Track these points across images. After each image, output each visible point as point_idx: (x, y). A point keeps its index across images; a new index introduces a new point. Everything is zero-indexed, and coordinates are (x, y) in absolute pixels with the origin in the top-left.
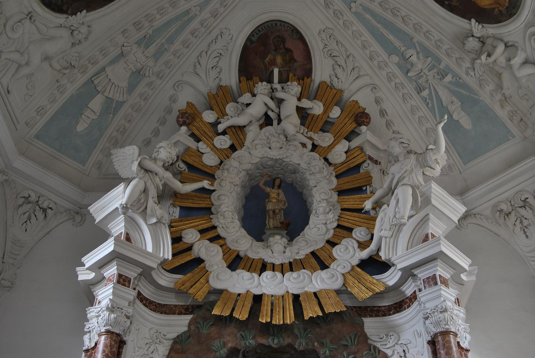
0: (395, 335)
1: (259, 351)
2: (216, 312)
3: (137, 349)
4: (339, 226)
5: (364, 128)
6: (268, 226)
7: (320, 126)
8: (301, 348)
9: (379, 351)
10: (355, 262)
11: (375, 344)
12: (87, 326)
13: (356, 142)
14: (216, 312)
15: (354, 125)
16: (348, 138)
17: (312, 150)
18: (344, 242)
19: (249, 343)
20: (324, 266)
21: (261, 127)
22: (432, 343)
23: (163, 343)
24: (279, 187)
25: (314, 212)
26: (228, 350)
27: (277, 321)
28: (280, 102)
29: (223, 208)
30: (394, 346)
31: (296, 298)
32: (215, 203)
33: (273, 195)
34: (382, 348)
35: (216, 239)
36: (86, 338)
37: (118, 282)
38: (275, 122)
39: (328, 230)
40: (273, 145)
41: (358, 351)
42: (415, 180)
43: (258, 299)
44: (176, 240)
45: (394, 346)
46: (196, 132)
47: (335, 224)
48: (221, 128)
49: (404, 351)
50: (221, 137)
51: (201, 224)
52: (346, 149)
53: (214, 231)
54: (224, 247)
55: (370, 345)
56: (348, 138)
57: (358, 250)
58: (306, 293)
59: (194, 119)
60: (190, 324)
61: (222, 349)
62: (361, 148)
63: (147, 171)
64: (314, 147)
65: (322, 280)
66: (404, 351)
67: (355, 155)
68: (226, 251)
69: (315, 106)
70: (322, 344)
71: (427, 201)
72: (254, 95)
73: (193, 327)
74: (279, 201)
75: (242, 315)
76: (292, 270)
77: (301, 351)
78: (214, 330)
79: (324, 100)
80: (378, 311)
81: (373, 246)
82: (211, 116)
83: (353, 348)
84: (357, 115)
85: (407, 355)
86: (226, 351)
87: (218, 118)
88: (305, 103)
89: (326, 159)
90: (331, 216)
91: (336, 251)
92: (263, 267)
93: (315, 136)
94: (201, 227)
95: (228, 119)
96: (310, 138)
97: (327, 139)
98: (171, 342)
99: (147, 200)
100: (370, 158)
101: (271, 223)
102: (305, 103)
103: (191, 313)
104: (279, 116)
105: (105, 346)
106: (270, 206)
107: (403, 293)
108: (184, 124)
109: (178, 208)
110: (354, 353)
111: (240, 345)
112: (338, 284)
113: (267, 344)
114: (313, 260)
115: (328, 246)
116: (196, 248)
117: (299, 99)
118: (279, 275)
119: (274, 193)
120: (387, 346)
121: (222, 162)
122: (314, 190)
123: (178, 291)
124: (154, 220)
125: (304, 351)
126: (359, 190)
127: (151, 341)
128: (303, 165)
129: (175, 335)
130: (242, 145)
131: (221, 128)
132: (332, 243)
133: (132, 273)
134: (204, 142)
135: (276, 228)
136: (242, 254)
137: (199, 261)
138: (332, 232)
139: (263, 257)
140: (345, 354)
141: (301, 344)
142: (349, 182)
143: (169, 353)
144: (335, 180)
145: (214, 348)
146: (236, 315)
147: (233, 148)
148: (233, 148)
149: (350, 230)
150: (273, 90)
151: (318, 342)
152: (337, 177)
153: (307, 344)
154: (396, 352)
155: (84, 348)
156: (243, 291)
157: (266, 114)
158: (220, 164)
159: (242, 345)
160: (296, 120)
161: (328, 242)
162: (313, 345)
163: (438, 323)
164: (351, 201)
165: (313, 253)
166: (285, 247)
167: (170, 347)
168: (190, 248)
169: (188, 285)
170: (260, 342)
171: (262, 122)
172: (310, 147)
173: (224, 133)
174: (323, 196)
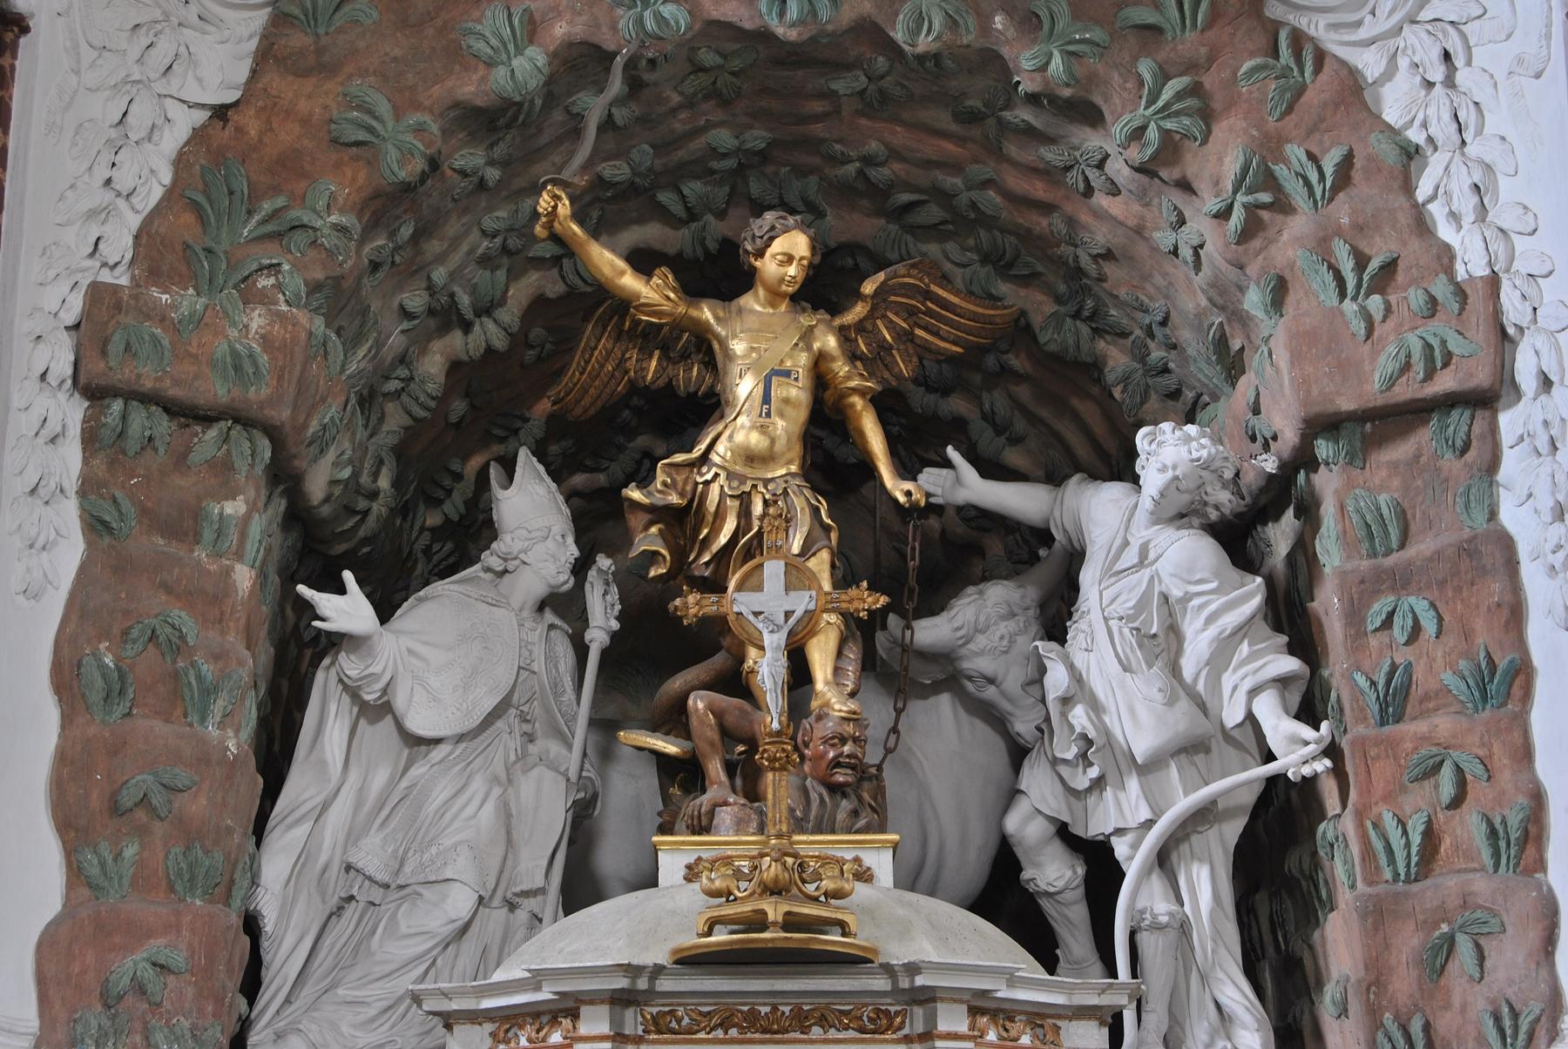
1: (708, 58)
3: (88, 55)
8: (925, 43)
9: (1320, 57)
11: (1303, 22)
19: (660, 19)
23: (219, 23)
26: (554, 56)
30: (1398, 30)
34: (1333, 43)
41: (1211, 59)
45: (1398, 30)
49: (1447, 56)
55: (1276, 26)
61: (519, 51)
66: (1447, 56)
77: (921, 58)
85: (1461, 77)
86: (541, 60)
110: (1190, 67)
111: (614, 28)
113: (748, 25)
120: (1363, 33)
125: (936, 57)
127: (158, 14)
140: (1145, 69)
143: (254, 73)
145: (480, 46)
151: (1009, 11)
153: (952, 23)
154: (1403, 62)
162: (985, 28)
167: (254, 43)
170: (715, 14)
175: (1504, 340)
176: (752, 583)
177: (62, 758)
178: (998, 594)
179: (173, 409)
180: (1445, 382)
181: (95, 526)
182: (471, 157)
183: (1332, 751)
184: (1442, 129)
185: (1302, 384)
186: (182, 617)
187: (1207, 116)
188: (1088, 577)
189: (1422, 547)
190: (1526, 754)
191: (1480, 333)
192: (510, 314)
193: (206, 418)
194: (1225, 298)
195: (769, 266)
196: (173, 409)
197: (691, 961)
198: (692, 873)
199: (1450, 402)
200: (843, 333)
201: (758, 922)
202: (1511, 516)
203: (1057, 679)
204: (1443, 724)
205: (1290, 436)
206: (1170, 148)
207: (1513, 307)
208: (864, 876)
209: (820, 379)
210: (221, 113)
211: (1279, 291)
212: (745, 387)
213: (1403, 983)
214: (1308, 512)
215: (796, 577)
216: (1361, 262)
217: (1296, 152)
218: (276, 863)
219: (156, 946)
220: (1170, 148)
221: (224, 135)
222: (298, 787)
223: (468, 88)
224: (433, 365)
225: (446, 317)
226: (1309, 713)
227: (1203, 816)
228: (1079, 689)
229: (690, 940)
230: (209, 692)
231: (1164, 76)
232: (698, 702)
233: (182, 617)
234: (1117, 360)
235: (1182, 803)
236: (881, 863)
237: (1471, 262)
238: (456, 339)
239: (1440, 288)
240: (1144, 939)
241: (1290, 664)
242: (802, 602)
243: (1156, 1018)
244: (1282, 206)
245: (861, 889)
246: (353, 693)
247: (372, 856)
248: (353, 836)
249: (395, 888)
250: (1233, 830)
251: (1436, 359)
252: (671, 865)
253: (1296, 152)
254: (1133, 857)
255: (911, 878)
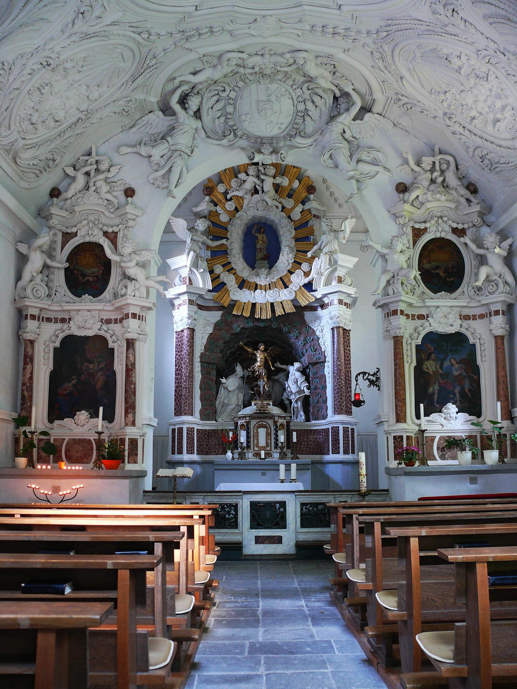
0: (319, 321)
2: (234, 312)
4: (295, 262)
5: (312, 196)
6: (257, 258)
7: (286, 194)
8: (275, 327)
9: (311, 328)
10: (302, 284)
12: (174, 320)
13: (307, 206)
14: (234, 312)
15: (306, 194)
16: (303, 203)
17: (282, 211)
18: (297, 271)
20: (286, 287)
21: (252, 195)
22: (333, 329)
24: (263, 233)
25: (282, 252)
27: (264, 317)
28: (262, 181)
29: (234, 252)
31: (272, 304)
32: (229, 247)
33: (260, 238)
34: (312, 327)
35: (231, 270)
36: (175, 326)
37: (189, 304)
38: (260, 192)
39: (289, 264)
40: (260, 209)
42: (333, 247)
43: (254, 305)
44: (211, 272)
46: (215, 200)
47: (293, 261)
48: (229, 197)
50: (229, 202)
51: (222, 262)
52: (301, 210)
53: (230, 265)
54: (236, 275)
56: (303, 203)
57: (303, 277)
58: (277, 302)
59: (213, 191)
60: (222, 317)
62: (309, 210)
63: (194, 241)
64: (283, 208)
65: (285, 295)
67: (306, 215)
68: (237, 277)
69: (284, 181)
70: (284, 325)
71: (336, 262)
72: (248, 175)
73: (223, 318)
74: (263, 242)
75: (247, 314)
76: (270, 289)
78: (233, 318)
79: (289, 176)
80: (312, 308)
81: (310, 277)
82: (222, 188)
83: (299, 327)
84: (308, 188)
87: (227, 189)
88: (279, 180)
89: (289, 217)
90: (290, 256)
91: (293, 277)
92: (256, 287)
93: (284, 201)
94: (223, 263)
95: (233, 191)
96: (281, 203)
97: (290, 203)
98: (214, 325)
99: (198, 261)
100: (315, 216)
101: (259, 255)
102: (279, 180)
103: (221, 310)
104: (263, 188)
105: (188, 334)
106: (258, 246)
107: (324, 301)
108: (208, 195)
109: (210, 251)
112: (292, 297)
114: (281, 282)
115: (289, 274)
116: (222, 276)
117: (274, 177)
118: (264, 292)
119: (260, 237)
121: (231, 219)
122: (282, 238)
123: (214, 300)
124: (202, 270)
126: (306, 239)
128: (277, 221)
129: (215, 321)
130: (242, 207)
131: (229, 197)
132: (291, 272)
133: (194, 298)
134: (220, 206)
135: (262, 259)
136: (245, 279)
137: (223, 284)
138: (291, 265)
139: (256, 281)
141: (274, 326)
142: (303, 233)
144: (293, 231)
146: (244, 314)
147: (237, 210)
148: (237, 210)
149: (300, 264)
150: (259, 170)
152: (296, 229)
155: (175, 331)
156: (246, 301)
157: (255, 186)
158: (230, 220)
159: (247, 325)
160: (273, 192)
161: (289, 271)
163: (335, 323)
164: (302, 246)
165: (281, 278)
166: (267, 275)
168: (219, 277)
169: (220, 298)
171: (252, 191)
172: (280, 209)
173: (231, 199)
174: (287, 243)
175: (325, 357)
176: (260, 381)
177: (201, 395)
178: (283, 374)
179: (208, 363)
180: (320, 361)
181: (202, 374)
182: (233, 337)
183: (310, 392)
184: (321, 336)
185: (308, 360)
186: (210, 382)
187: (300, 334)
188: (290, 375)
189: (318, 375)
190: (326, 394)
191: (323, 356)
192: (236, 348)
193: (211, 364)
194: (302, 349)
195: (261, 348)
196: (208, 363)
197: (255, 413)
198: (255, 404)
199: (321, 362)
200: (267, 353)
201: (261, 410)
202: (326, 373)
203: (287, 385)
204: (319, 391)
205: (307, 364)
206: (297, 337)
207: (326, 355)
208: (270, 405)
209: (265, 358)
210: (211, 334)
211: (307, 351)
212: (259, 359)
213: (315, 413)
214: (310, 369)
215: (264, 381)
216: (314, 348)
217: (308, 338)
218: (217, 403)
219: (209, 411)
220: (297, 337)
221: (211, 336)
222: (219, 396)
223: (233, 332)
224: (228, 352)
225: (230, 348)
226: (308, 389)
227: (299, 397)
228: (289, 387)
229: (255, 412)
230: (212, 388)
231: (296, 330)
232: (255, 389)
233: (210, 382)
234: (294, 352)
235: (298, 397)
236: (271, 403)
237: (323, 350)
238: (230, 350)
239: (320, 352)
240: (295, 409)
241: (307, 384)
242: (264, 383)
243: (295, 415)
244: (307, 343)
245: (269, 406)
246: (224, 387)
247: (226, 401)
248: (224, 400)
249: (228, 405)
250: (302, 399)
251: (320, 358)
252: (253, 404)
253: (308, 338)
254: (293, 401)
255: (274, 405)
